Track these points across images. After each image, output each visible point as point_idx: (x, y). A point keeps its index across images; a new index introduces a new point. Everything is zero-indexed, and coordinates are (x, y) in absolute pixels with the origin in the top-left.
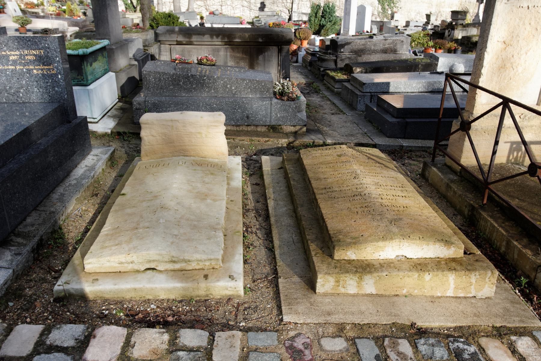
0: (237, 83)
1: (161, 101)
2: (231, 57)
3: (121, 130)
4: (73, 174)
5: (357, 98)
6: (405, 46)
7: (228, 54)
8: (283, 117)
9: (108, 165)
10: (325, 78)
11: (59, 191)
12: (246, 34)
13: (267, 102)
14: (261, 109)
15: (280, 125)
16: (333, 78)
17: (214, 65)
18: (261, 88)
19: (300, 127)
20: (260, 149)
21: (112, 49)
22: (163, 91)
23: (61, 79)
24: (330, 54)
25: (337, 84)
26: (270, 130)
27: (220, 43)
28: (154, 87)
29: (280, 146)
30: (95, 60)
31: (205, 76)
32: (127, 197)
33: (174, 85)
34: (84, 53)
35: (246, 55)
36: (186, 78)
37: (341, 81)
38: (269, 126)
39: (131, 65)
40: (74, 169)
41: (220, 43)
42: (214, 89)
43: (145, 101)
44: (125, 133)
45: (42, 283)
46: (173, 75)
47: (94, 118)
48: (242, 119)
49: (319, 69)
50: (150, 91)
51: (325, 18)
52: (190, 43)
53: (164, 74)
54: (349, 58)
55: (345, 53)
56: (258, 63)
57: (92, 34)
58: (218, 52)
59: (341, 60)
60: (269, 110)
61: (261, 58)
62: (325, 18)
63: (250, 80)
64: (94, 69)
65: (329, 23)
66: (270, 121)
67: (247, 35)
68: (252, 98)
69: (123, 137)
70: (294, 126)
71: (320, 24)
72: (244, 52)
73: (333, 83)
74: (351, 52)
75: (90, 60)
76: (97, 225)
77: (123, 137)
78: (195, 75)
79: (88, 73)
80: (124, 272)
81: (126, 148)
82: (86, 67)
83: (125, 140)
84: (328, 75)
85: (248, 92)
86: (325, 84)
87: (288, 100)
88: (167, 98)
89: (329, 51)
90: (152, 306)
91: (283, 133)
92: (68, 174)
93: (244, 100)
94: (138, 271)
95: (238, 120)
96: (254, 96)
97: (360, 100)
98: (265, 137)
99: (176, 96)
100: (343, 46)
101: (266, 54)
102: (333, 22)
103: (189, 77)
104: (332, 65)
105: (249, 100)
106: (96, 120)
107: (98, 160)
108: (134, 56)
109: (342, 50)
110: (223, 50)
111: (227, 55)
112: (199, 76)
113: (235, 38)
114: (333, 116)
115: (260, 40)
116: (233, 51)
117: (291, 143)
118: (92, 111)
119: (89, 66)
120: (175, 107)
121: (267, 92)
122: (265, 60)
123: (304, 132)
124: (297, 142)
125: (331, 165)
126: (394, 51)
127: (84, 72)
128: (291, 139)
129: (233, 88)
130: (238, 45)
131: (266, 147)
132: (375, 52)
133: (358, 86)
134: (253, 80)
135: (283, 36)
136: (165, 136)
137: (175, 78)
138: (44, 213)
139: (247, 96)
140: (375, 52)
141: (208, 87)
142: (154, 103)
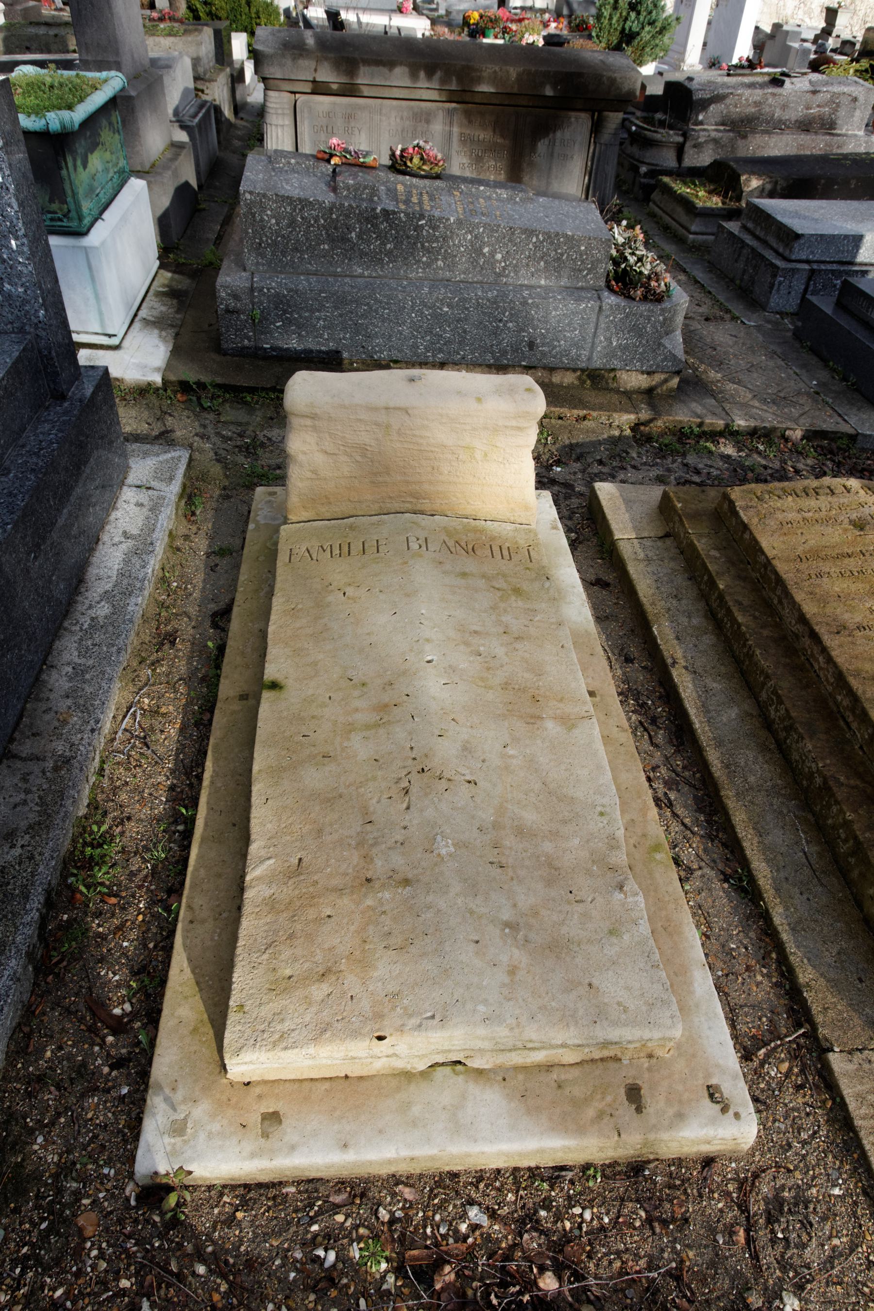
0: (510, 240)
1: (296, 291)
2: (465, 140)
3: (191, 375)
4: (92, 572)
5: (774, 276)
6: (858, 113)
7: (456, 130)
8: (625, 348)
9: (180, 512)
10: (656, 196)
11: (66, 657)
12: (511, 70)
13: (588, 305)
14: (569, 324)
15: (613, 370)
16: (687, 204)
17: (438, 177)
18: (555, 251)
19: (663, 377)
20: (567, 442)
21: (129, 98)
22: (301, 259)
23: (20, 253)
24: (662, 124)
25: (698, 220)
26: (585, 382)
27: (434, 95)
28: (275, 243)
29: (617, 433)
30: (94, 146)
31: (422, 217)
32: (293, 696)
33: (333, 240)
34: (63, 126)
35: (502, 136)
36: (368, 220)
37: (708, 214)
38: (583, 370)
39: (177, 146)
40: (92, 550)
41: (434, 95)
42: (445, 258)
43: (252, 289)
44: (201, 385)
45: (83, 1096)
46: (331, 209)
47: (110, 336)
48: (516, 350)
49: (636, 169)
50: (263, 256)
51: (638, 13)
52: (349, 91)
53: (304, 203)
54: (715, 141)
55: (708, 124)
56: (531, 164)
57: (52, 32)
58: (428, 122)
59: (695, 146)
60: (592, 325)
61: (542, 146)
62: (638, 13)
63: (548, 235)
64: (93, 178)
65: (647, 28)
66: (590, 359)
67: (513, 72)
68: (547, 289)
69: (199, 398)
70: (649, 373)
71: (623, 29)
72: (498, 126)
73: (683, 218)
74: (723, 124)
75: (80, 146)
76: (210, 809)
77: (199, 398)
78: (394, 213)
79: (81, 192)
80: (361, 1078)
81: (214, 439)
82: (73, 176)
83: (203, 409)
84: (668, 191)
85: (538, 270)
86: (652, 215)
87: (645, 298)
88: (313, 279)
89: (659, 116)
90: (474, 1213)
91: (617, 391)
92: (77, 580)
93: (526, 293)
94: (407, 1076)
95: (504, 353)
96: (551, 283)
97: (780, 283)
98: (575, 408)
99: (335, 275)
100: (704, 104)
101: (559, 134)
102: (659, 25)
103: (376, 217)
104: (668, 159)
105: (539, 295)
106: (115, 341)
107: (155, 508)
108: (176, 113)
109: (701, 117)
110: (440, 115)
111: (450, 133)
112: (407, 215)
113: (479, 80)
114: (712, 327)
115: (549, 92)
116: (470, 122)
117: (642, 424)
118: (101, 313)
119: (80, 169)
120: (336, 308)
121: (590, 271)
122: (552, 155)
123: (671, 390)
124: (660, 423)
125: (851, 564)
126: (827, 126)
127: (69, 192)
128: (645, 414)
129: (499, 256)
130: (486, 101)
131: (581, 438)
132: (778, 126)
133: (773, 242)
134: (557, 234)
135: (613, 81)
136: (364, 456)
137: (337, 220)
138: (35, 767)
139: (534, 281)
140: (778, 126)
141: (429, 251)
142: (277, 295)
